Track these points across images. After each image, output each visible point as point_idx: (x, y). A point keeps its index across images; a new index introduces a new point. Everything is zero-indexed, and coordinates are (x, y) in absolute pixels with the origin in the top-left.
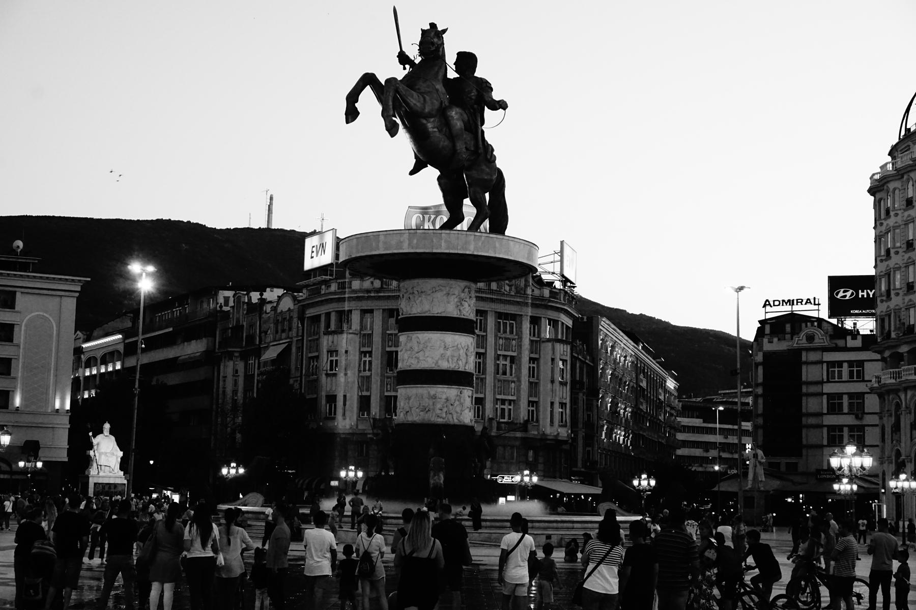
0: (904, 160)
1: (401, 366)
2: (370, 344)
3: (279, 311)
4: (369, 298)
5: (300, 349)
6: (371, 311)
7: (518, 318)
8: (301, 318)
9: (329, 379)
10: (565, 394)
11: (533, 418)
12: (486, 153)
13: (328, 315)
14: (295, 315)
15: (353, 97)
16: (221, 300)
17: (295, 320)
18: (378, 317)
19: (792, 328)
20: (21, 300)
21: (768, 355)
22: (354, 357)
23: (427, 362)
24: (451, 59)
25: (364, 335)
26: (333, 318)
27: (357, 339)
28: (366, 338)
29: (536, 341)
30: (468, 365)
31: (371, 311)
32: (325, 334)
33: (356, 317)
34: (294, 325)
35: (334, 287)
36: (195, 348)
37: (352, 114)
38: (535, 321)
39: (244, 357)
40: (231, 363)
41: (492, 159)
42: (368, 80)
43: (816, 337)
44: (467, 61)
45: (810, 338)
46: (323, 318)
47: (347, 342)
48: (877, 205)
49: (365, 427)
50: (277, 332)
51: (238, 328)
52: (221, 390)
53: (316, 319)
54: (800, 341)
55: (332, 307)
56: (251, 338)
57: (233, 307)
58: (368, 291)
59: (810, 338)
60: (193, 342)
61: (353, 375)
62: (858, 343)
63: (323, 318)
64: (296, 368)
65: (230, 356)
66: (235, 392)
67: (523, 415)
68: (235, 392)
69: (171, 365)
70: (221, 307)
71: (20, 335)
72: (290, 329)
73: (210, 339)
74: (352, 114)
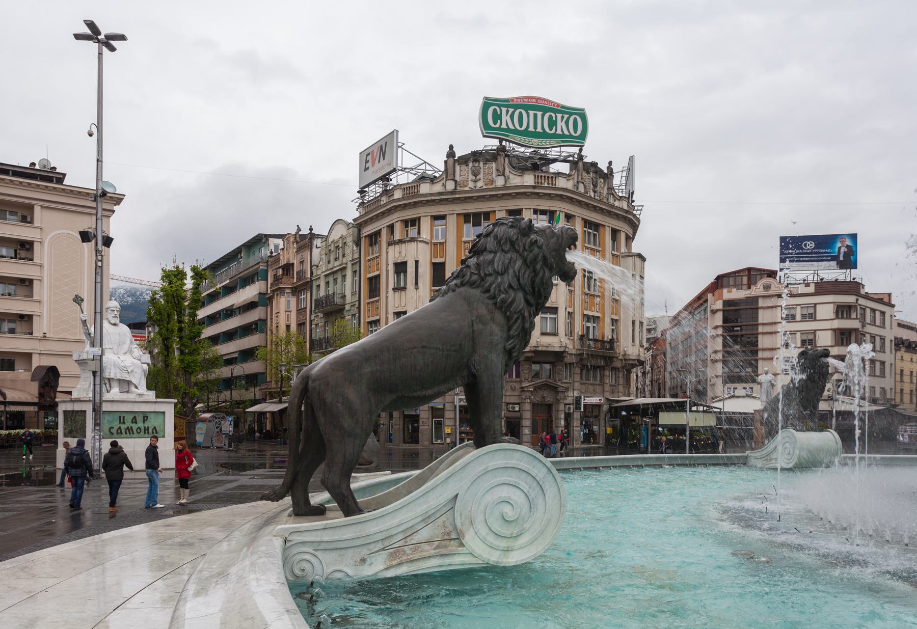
2: (443, 254)
3: (331, 240)
4: (441, 201)
6: (443, 217)
7: (601, 229)
9: (397, 293)
13: (391, 228)
14: (349, 240)
16: (272, 247)
17: (351, 244)
18: (452, 221)
19: (749, 280)
21: (727, 303)
25: (435, 244)
26: (398, 228)
27: (427, 248)
28: (438, 247)
29: (617, 256)
31: (443, 217)
32: (390, 244)
33: (425, 224)
34: (348, 250)
38: (615, 233)
43: (773, 286)
45: (767, 287)
46: (384, 233)
50: (329, 262)
51: (288, 268)
52: (274, 325)
54: (757, 289)
56: (301, 273)
57: (283, 249)
58: (440, 194)
59: (767, 287)
60: (247, 287)
62: (811, 289)
63: (384, 233)
64: (353, 294)
65: (281, 291)
66: (288, 327)
68: (288, 327)
69: (229, 313)
70: (271, 253)
72: (344, 256)
73: (263, 282)
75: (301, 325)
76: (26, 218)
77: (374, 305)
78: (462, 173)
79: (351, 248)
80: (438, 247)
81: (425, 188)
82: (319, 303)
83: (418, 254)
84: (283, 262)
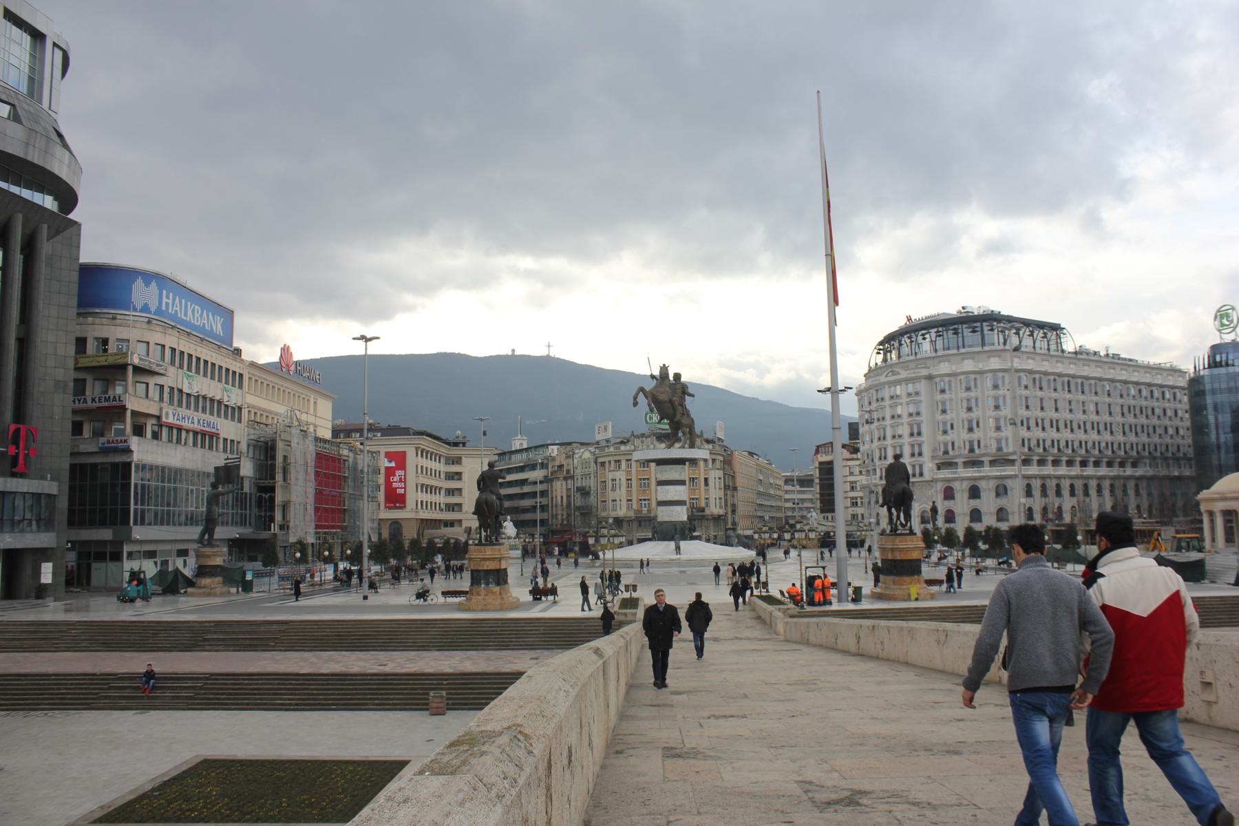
0: (871, 382)
1: (660, 499)
5: (596, 477)
8: (596, 462)
10: (721, 494)
11: (707, 505)
12: (686, 413)
15: (635, 398)
20: (464, 460)
21: (820, 463)
22: (624, 482)
23: (669, 498)
24: (671, 378)
28: (629, 473)
30: (685, 497)
33: (623, 464)
35: (612, 449)
36: (537, 474)
37: (635, 404)
39: (565, 479)
40: (559, 483)
41: (689, 415)
42: (642, 390)
44: (677, 376)
47: (621, 475)
48: (859, 400)
49: (632, 514)
51: (561, 466)
53: (603, 464)
55: (611, 458)
56: (568, 471)
61: (624, 489)
67: (703, 505)
69: (523, 482)
71: (465, 477)
74: (635, 404)
75: (569, 497)
76: (457, 461)
77: (603, 494)
78: (637, 442)
79: (593, 464)
80: (629, 473)
81: (623, 448)
82: (579, 489)
83: (621, 475)
84: (557, 463)
